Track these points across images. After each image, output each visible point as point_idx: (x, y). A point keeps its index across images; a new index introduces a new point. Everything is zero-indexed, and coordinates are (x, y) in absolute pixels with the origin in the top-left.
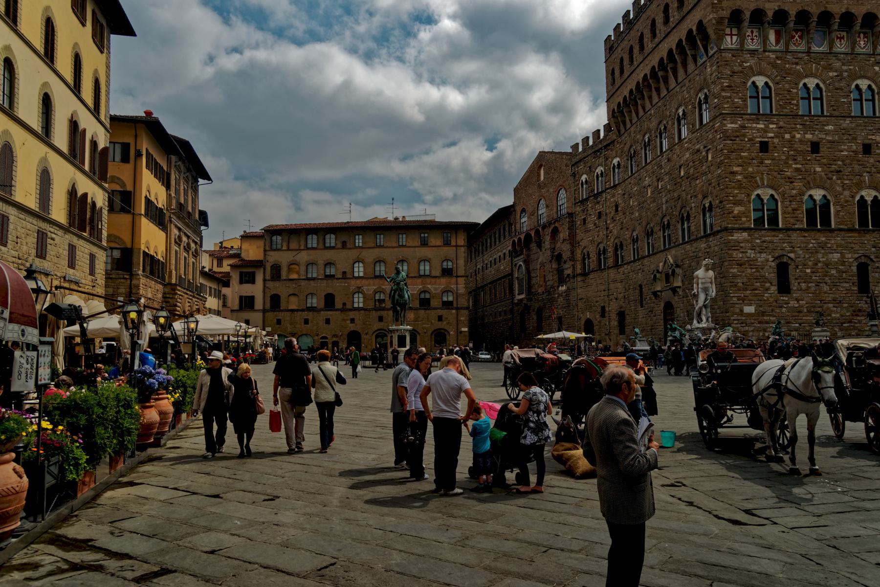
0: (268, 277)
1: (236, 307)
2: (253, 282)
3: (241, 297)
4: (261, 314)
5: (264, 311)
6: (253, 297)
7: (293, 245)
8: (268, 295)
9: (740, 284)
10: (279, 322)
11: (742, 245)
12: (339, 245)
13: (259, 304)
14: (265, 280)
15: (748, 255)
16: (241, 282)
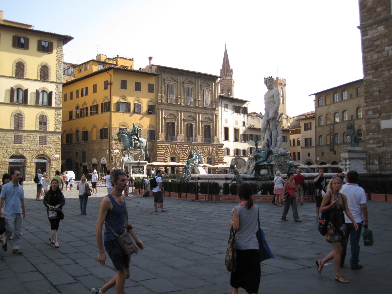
0: (317, 125)
1: (304, 146)
2: (310, 129)
3: (306, 139)
4: (315, 149)
5: (316, 147)
6: (311, 139)
7: (328, 102)
8: (318, 136)
9: (377, 93)
10: (323, 154)
11: (377, 43)
12: (349, 97)
13: (314, 144)
14: (316, 127)
15: (385, 53)
16: (305, 130)
